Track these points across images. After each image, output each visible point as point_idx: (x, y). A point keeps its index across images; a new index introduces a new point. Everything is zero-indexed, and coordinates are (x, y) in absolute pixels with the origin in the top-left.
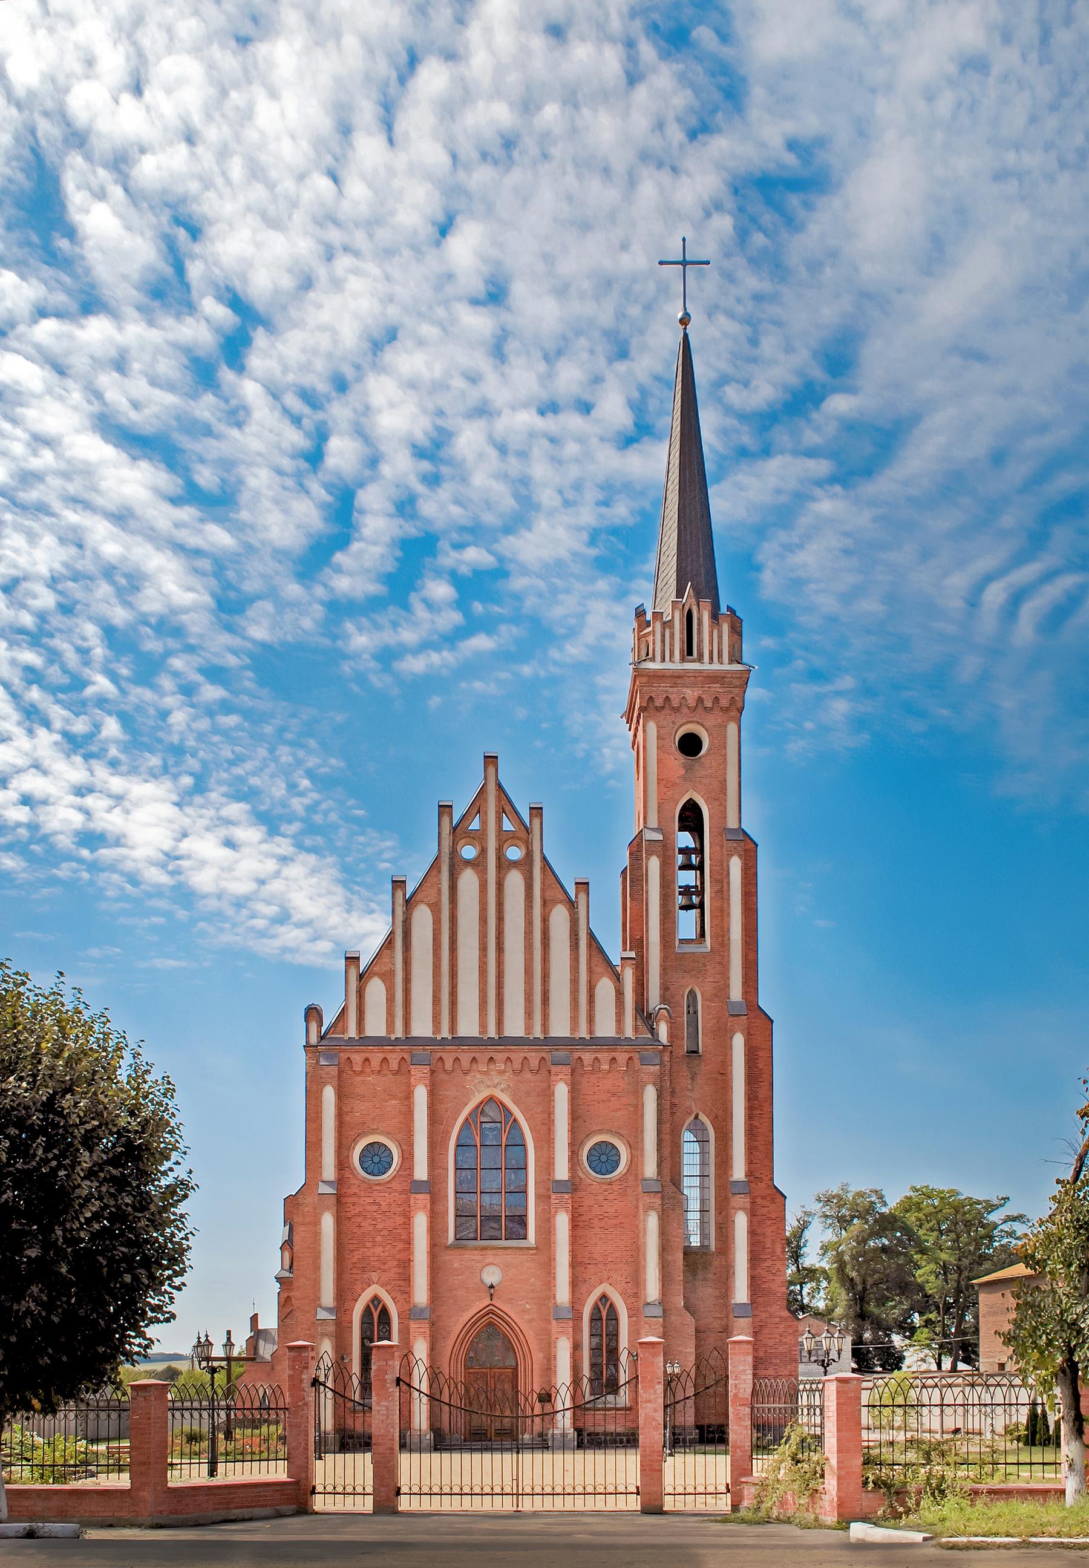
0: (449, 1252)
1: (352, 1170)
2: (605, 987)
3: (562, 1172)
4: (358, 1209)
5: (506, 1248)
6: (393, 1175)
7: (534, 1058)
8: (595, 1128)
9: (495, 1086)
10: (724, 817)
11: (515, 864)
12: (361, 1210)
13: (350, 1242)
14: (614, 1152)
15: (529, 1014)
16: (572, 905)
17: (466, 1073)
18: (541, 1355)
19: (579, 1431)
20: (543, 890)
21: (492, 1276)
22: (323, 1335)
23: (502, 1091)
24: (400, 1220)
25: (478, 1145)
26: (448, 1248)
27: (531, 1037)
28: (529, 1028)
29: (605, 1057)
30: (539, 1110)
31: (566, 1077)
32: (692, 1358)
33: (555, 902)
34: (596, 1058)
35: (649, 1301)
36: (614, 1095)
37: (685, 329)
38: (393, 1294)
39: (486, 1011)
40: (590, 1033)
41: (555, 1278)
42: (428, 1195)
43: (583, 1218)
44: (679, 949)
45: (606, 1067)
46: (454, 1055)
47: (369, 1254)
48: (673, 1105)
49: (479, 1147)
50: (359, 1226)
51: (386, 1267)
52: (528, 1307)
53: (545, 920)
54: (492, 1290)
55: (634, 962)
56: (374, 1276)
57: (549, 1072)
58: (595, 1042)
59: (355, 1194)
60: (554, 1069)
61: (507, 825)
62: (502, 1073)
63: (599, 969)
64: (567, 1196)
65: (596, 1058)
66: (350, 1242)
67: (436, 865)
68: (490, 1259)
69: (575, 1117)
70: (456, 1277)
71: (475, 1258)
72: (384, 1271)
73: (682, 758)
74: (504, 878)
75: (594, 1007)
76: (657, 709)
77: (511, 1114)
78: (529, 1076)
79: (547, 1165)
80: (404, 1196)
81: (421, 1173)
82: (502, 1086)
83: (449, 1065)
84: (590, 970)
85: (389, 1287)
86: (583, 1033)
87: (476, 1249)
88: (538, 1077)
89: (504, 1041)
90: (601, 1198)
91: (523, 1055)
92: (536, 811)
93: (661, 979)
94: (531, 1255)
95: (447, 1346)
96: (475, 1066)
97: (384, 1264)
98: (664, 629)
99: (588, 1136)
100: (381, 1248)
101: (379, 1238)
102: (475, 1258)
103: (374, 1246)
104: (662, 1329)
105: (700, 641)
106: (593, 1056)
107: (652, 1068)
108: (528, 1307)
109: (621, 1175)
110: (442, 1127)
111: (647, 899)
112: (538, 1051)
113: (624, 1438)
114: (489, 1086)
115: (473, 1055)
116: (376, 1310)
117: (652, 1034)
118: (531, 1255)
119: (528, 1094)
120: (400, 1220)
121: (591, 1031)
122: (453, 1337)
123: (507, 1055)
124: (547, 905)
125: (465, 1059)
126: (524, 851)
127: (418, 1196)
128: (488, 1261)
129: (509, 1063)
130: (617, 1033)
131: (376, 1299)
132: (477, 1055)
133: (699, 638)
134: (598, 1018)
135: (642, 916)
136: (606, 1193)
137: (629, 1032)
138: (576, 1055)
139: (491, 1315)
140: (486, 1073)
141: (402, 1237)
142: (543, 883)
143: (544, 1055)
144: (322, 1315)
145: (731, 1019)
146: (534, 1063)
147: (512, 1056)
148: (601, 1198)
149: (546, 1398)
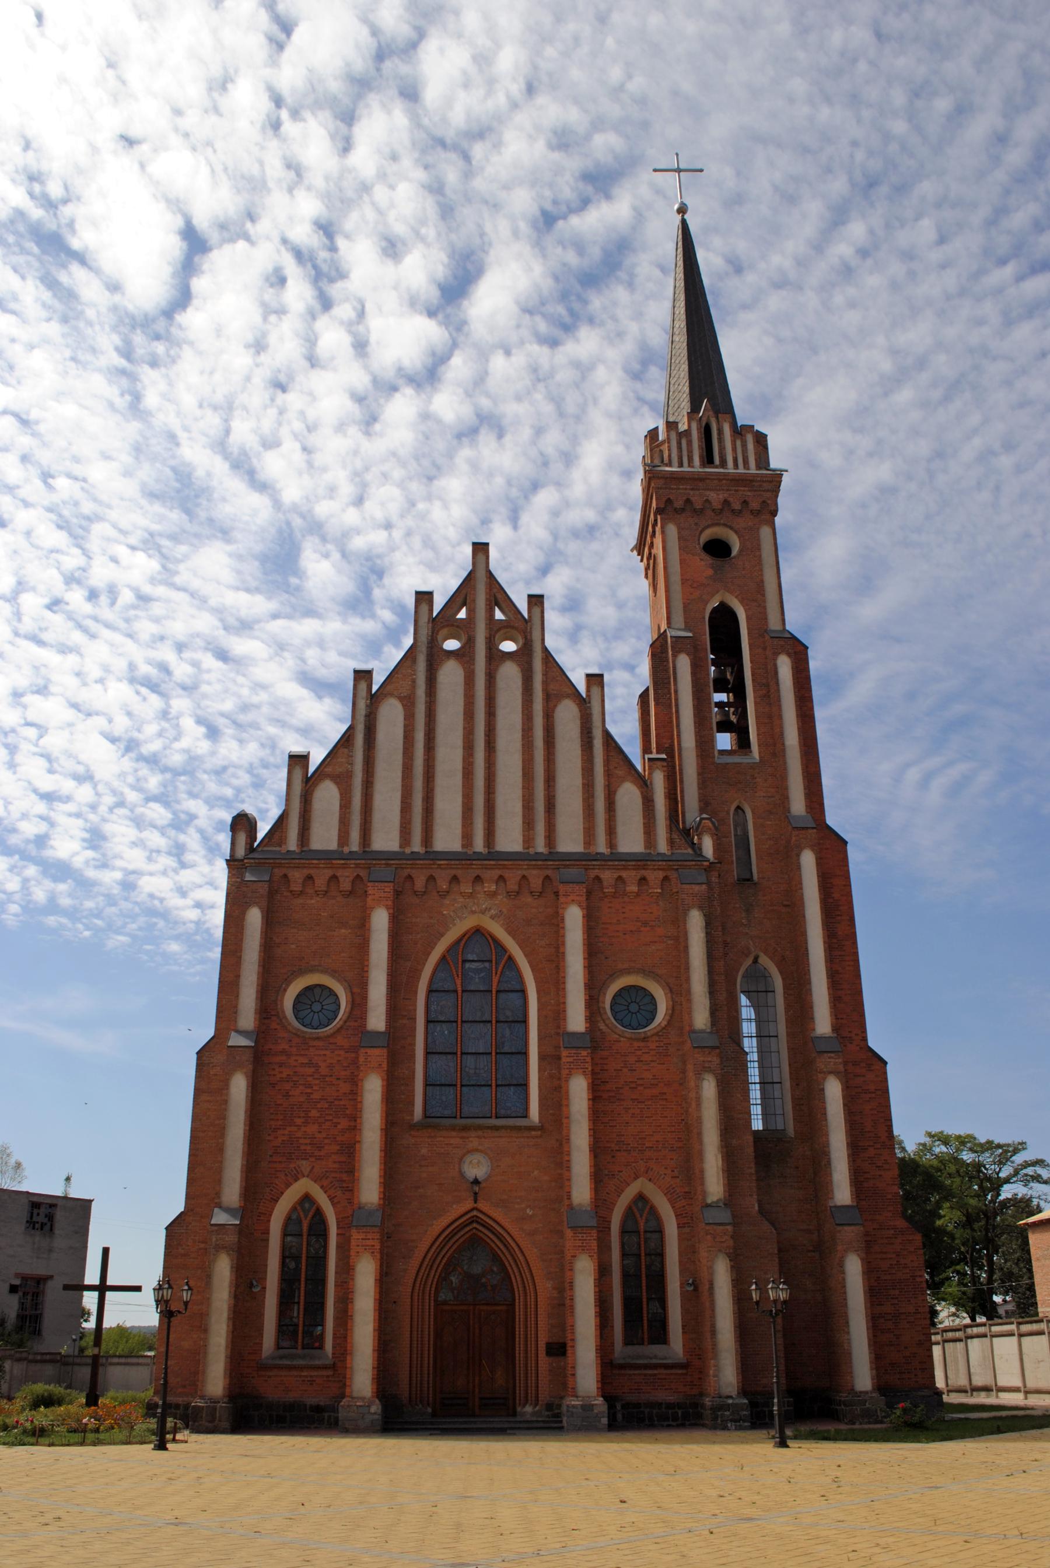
1: (280, 1016)
2: (629, 795)
3: (576, 1020)
5: (496, 1128)
6: (338, 1026)
9: (483, 912)
10: (764, 618)
11: (510, 655)
12: (292, 1073)
13: (272, 1117)
14: (647, 1000)
15: (528, 824)
16: (583, 703)
17: (444, 894)
18: (549, 1285)
19: (610, 1399)
20: (545, 683)
21: (476, 1168)
22: (219, 1248)
23: (492, 917)
24: (345, 1088)
25: (459, 989)
26: (414, 1127)
27: (531, 851)
28: (528, 839)
29: (631, 876)
31: (578, 898)
33: (560, 697)
34: (620, 878)
35: (709, 1201)
36: (645, 924)
39: (472, 819)
41: (569, 1169)
42: (385, 1050)
44: (720, 760)
45: (633, 888)
47: (299, 1134)
48: (726, 944)
49: (460, 992)
50: (287, 1095)
52: (529, 1212)
54: (476, 1189)
55: (665, 764)
56: (305, 1165)
57: (557, 894)
58: (616, 859)
59: (284, 1052)
60: (562, 889)
62: (493, 895)
63: (620, 772)
64: (584, 1053)
65: (620, 878)
66: (272, 1117)
67: (410, 654)
68: (474, 1143)
69: (592, 952)
71: (452, 1141)
75: (614, 816)
76: (676, 510)
77: (504, 950)
78: (529, 899)
80: (353, 1055)
81: (377, 1020)
82: (493, 912)
83: (420, 883)
84: (608, 774)
86: (601, 847)
87: (453, 1128)
89: (493, 857)
92: (536, 601)
93: (699, 788)
97: (320, 1148)
99: (613, 976)
100: (316, 1126)
101: (314, 1113)
102: (452, 1141)
104: (731, 1243)
106: (616, 875)
107: (696, 888)
108: (529, 1212)
109: (659, 1029)
111: (677, 700)
112: (539, 867)
113: (680, 1412)
114: (474, 912)
115: (453, 872)
116: (306, 1217)
117: (693, 849)
118: (533, 1137)
120: (345, 1088)
121: (611, 843)
122: (419, 1254)
123: (498, 872)
124: (551, 701)
126: (521, 642)
127: (370, 1051)
129: (502, 884)
130: (646, 847)
131: (307, 1198)
134: (620, 829)
135: (671, 722)
136: (639, 1053)
137: (663, 847)
138: (593, 874)
139: (475, 1225)
140: (471, 895)
141: (348, 1112)
142: (545, 674)
143: (549, 872)
144: (220, 1218)
145: (795, 833)
146: (536, 883)
147: (507, 874)
149: (559, 1349)
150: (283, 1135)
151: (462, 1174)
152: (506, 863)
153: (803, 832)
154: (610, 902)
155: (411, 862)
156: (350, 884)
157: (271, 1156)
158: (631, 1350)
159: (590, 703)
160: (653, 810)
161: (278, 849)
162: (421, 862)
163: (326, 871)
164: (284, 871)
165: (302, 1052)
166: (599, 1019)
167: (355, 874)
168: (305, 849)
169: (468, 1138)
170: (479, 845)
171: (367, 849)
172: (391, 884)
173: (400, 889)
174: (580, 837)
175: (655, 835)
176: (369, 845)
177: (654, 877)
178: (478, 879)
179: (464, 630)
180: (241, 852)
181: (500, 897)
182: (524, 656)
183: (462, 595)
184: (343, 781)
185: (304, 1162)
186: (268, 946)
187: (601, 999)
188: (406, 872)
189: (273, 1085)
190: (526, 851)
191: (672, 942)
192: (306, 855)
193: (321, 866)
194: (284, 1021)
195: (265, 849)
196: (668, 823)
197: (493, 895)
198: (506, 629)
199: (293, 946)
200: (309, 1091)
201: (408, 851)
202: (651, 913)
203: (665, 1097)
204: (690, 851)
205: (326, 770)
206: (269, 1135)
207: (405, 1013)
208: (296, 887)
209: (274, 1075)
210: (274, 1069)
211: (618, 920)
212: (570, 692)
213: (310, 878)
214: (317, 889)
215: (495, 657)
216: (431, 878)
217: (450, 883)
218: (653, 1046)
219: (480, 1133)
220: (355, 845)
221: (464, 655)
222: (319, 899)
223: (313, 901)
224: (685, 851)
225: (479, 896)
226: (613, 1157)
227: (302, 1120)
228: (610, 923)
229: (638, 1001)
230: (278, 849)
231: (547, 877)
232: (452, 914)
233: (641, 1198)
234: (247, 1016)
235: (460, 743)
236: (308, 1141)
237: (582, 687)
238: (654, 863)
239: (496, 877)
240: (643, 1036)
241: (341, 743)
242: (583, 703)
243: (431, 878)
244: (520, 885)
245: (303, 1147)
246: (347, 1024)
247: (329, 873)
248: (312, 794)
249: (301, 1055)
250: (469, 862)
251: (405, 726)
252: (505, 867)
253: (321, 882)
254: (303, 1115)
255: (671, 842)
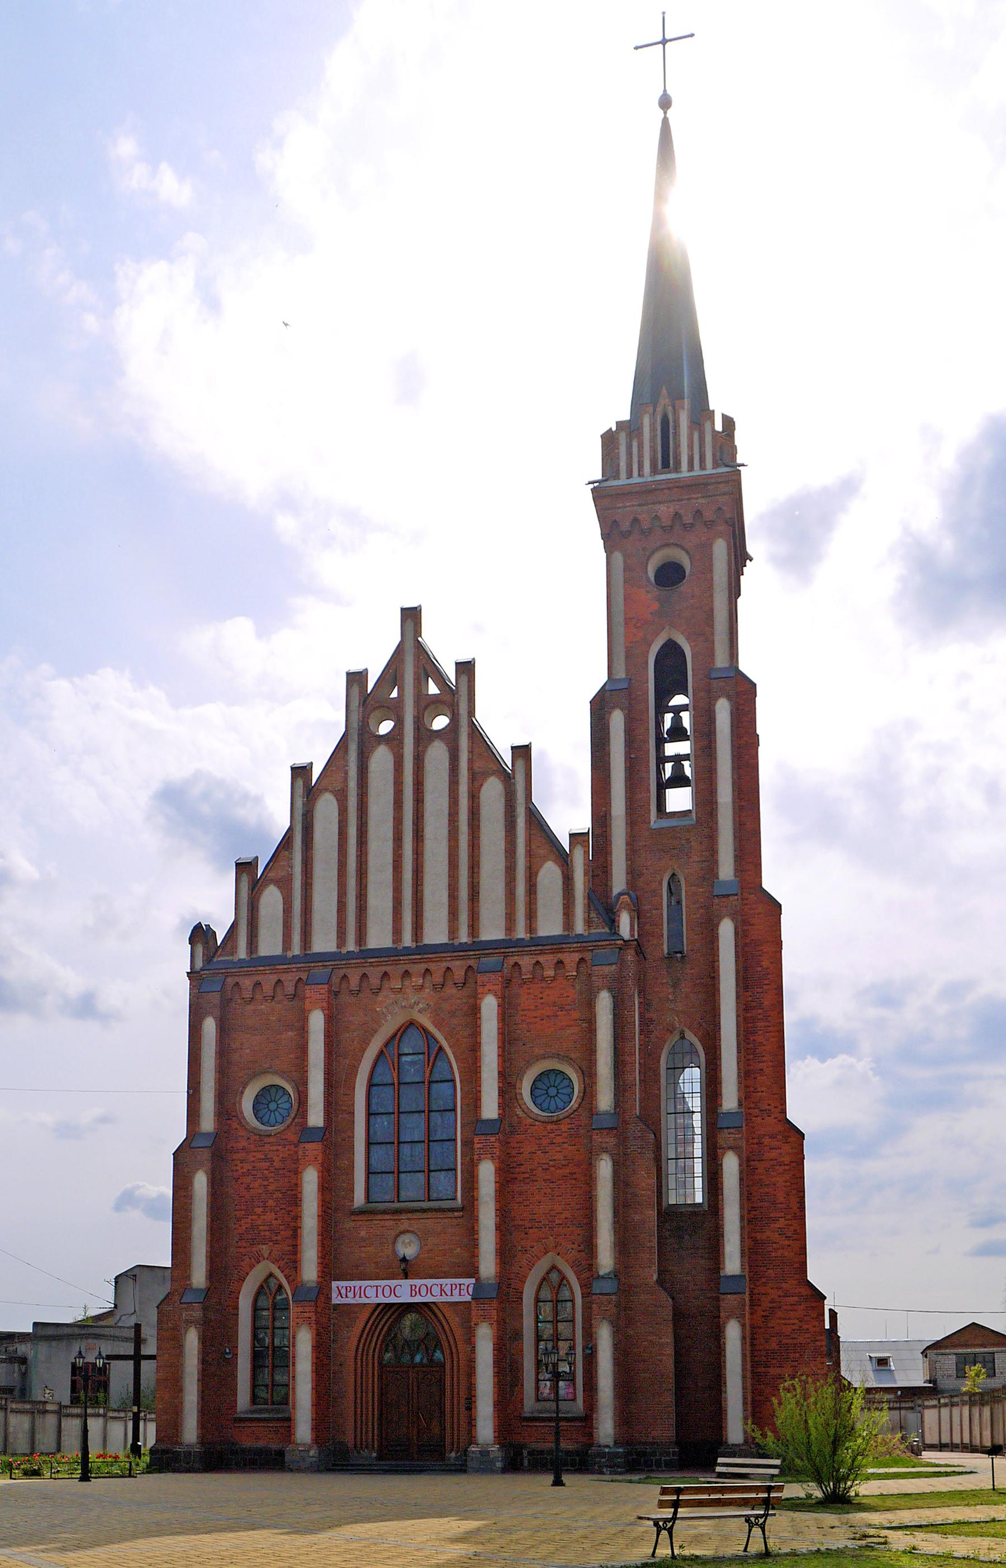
0: (353, 1217)
1: (239, 1116)
2: (550, 873)
4: (247, 1166)
7: (459, 968)
8: (537, 1051)
12: (251, 1168)
16: (507, 778)
20: (471, 761)
27: (456, 942)
28: (453, 931)
29: (548, 960)
30: (466, 1033)
32: (670, 1351)
33: (486, 775)
36: (562, 1009)
37: (665, 113)
38: (287, 1272)
39: (401, 914)
40: (531, 932)
43: (522, 1169)
45: (550, 973)
46: (361, 971)
47: (259, 1222)
50: (248, 1188)
51: (279, 1238)
53: (474, 797)
56: (265, 1249)
58: (538, 944)
61: (433, 689)
68: (405, 1225)
70: (363, 1249)
71: (387, 1223)
72: (276, 1242)
73: (656, 591)
74: (424, 752)
78: (454, 991)
79: (474, 1101)
81: (316, 1118)
83: (354, 981)
84: (529, 854)
85: (282, 1263)
86: (521, 933)
88: (465, 992)
89: (423, 951)
90: (545, 1142)
91: (444, 964)
94: (455, 1218)
95: (352, 1336)
96: (386, 985)
97: (277, 1235)
98: (631, 441)
101: (271, 1202)
103: (264, 1212)
105: (677, 446)
106: (534, 961)
110: (347, 1061)
119: (452, 1014)
121: (531, 928)
124: (476, 780)
125: (375, 975)
128: (402, 1228)
132: (388, 969)
133: (675, 443)
134: (541, 912)
137: (580, 928)
142: (471, 752)
143: (471, 962)
146: (459, 974)
147: (432, 966)
148: (545, 1142)
150: (246, 1223)
151: (394, 1252)
152: (430, 956)
153: (724, 900)
154: (529, 989)
155: (344, 962)
156: (293, 988)
157: (237, 1242)
158: (540, 1405)
159: (514, 778)
160: (573, 889)
161: (230, 958)
162: (354, 961)
163: (271, 977)
164: (237, 980)
165: (259, 1149)
166: (516, 1104)
167: (297, 978)
168: (254, 956)
169: (399, 1220)
170: (407, 940)
171: (309, 952)
172: (326, 986)
173: (337, 990)
174: (502, 923)
175: (573, 915)
176: (310, 947)
177: (571, 959)
178: (407, 974)
179: (394, 710)
180: (199, 964)
181: (427, 991)
182: (450, 734)
183: (392, 672)
184: (285, 885)
185: (264, 1247)
186: (223, 1052)
187: (517, 1084)
188: (342, 972)
189: (237, 1180)
190: (451, 942)
191: (586, 1025)
192: (257, 963)
193: (267, 972)
194: (242, 1121)
195: (220, 959)
196: (586, 901)
197: (422, 987)
198: (435, 705)
199: (248, 1051)
200: (266, 1183)
201: (344, 951)
202: (567, 996)
203: (575, 1176)
204: (607, 930)
205: (269, 875)
206: (235, 1224)
207: (344, 1108)
208: (247, 995)
209: (237, 1170)
210: (236, 1165)
211: (536, 1006)
212: (495, 768)
213: (258, 984)
214: (265, 995)
215: (424, 736)
216: (364, 976)
217: (382, 978)
218: (564, 1127)
219: (410, 1215)
220: (296, 950)
221: (393, 739)
222: (268, 1004)
223: (263, 1007)
224: (604, 931)
225: (407, 990)
226: (526, 1234)
227: (261, 1209)
228: (529, 1010)
229: (552, 1084)
230: (230, 958)
231: (470, 966)
232: (384, 1010)
233: (554, 1268)
234: (208, 1123)
235: (390, 835)
236: (267, 1228)
237: (507, 758)
238: (569, 945)
239: (423, 971)
240: (555, 1119)
241: (282, 845)
242: (507, 778)
243: (364, 976)
244: (444, 977)
245: (262, 1233)
246: (296, 1120)
247: (274, 978)
248: (258, 901)
249: (258, 1151)
250: (397, 958)
251: (340, 822)
252: (430, 960)
253: (268, 988)
254: (261, 1204)
255: (588, 922)
